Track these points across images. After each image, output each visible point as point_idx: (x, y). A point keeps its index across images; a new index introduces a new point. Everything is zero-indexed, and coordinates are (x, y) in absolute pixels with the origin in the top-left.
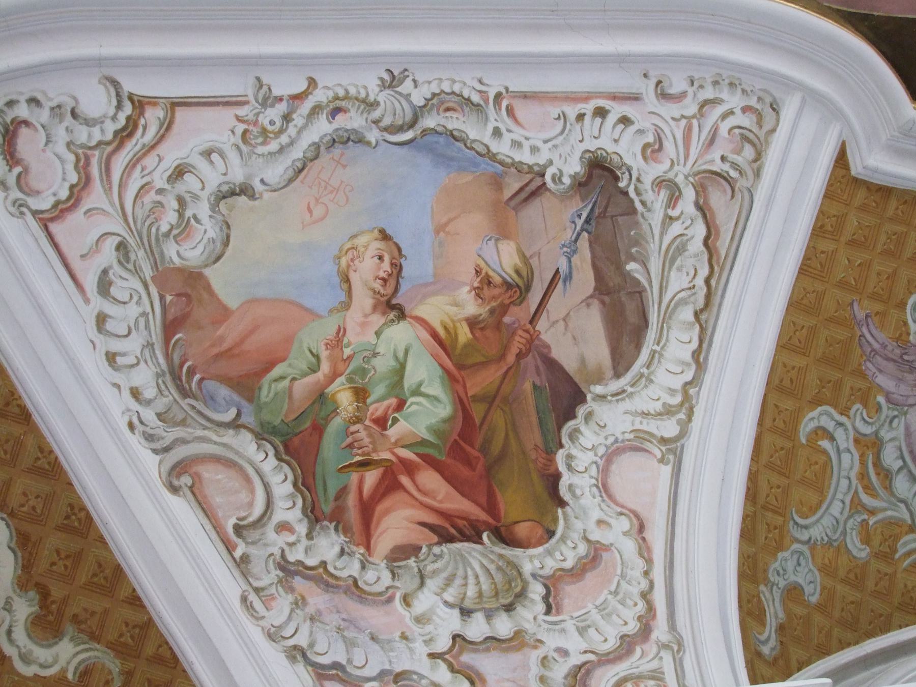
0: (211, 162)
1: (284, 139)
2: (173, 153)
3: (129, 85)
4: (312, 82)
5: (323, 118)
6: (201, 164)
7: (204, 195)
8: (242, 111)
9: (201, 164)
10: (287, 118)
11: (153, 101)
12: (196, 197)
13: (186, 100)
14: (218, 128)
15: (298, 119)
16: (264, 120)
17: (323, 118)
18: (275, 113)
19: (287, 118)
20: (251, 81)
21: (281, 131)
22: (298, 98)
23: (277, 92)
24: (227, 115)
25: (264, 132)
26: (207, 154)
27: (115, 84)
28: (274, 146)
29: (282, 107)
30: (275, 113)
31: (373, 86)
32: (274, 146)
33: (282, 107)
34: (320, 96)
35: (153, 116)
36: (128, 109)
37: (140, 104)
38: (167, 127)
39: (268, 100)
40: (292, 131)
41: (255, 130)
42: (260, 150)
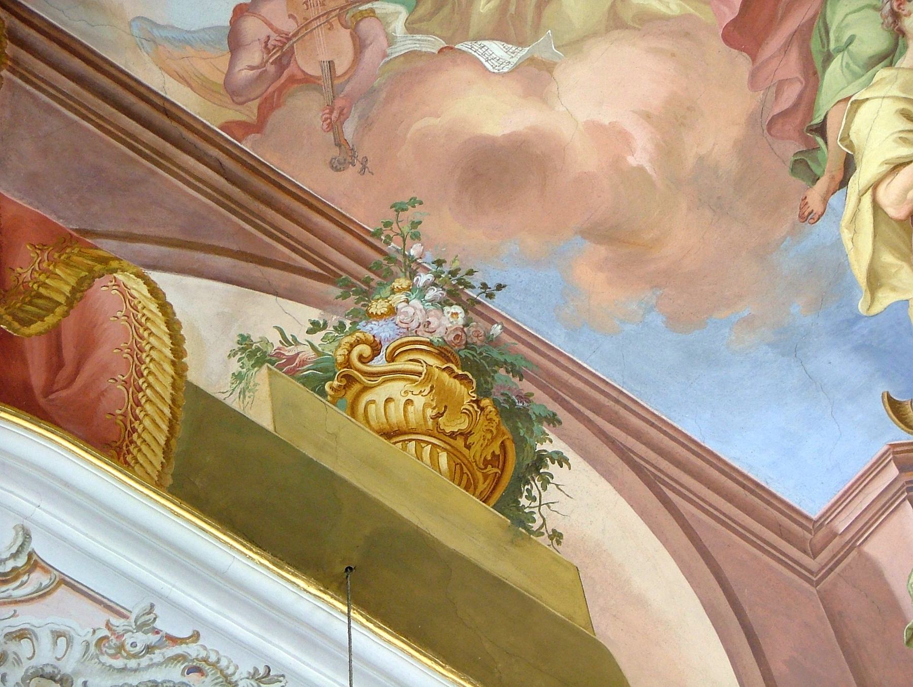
0: (55, 643)
1: (132, 663)
2: (26, 617)
3: (38, 545)
4: (196, 636)
5: (180, 667)
6: (45, 640)
7: (27, 664)
8: (115, 621)
9: (45, 640)
10: (149, 649)
11: (47, 568)
12: (18, 661)
13: (76, 584)
14: (84, 621)
15: (157, 656)
16: (128, 639)
17: (180, 667)
18: (142, 639)
19: (149, 649)
20: (145, 604)
21: (135, 656)
22: (174, 640)
23: (158, 625)
24: (100, 617)
25: (122, 647)
26: (57, 635)
27: (27, 536)
28: (119, 663)
29: (153, 639)
30: (142, 639)
31: (245, 668)
32: (119, 663)
33: (153, 639)
34: (193, 650)
35: (38, 579)
36: (21, 561)
37: (34, 564)
38: (42, 594)
39: (144, 626)
40: (145, 661)
41: (114, 641)
42: (105, 659)
